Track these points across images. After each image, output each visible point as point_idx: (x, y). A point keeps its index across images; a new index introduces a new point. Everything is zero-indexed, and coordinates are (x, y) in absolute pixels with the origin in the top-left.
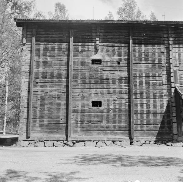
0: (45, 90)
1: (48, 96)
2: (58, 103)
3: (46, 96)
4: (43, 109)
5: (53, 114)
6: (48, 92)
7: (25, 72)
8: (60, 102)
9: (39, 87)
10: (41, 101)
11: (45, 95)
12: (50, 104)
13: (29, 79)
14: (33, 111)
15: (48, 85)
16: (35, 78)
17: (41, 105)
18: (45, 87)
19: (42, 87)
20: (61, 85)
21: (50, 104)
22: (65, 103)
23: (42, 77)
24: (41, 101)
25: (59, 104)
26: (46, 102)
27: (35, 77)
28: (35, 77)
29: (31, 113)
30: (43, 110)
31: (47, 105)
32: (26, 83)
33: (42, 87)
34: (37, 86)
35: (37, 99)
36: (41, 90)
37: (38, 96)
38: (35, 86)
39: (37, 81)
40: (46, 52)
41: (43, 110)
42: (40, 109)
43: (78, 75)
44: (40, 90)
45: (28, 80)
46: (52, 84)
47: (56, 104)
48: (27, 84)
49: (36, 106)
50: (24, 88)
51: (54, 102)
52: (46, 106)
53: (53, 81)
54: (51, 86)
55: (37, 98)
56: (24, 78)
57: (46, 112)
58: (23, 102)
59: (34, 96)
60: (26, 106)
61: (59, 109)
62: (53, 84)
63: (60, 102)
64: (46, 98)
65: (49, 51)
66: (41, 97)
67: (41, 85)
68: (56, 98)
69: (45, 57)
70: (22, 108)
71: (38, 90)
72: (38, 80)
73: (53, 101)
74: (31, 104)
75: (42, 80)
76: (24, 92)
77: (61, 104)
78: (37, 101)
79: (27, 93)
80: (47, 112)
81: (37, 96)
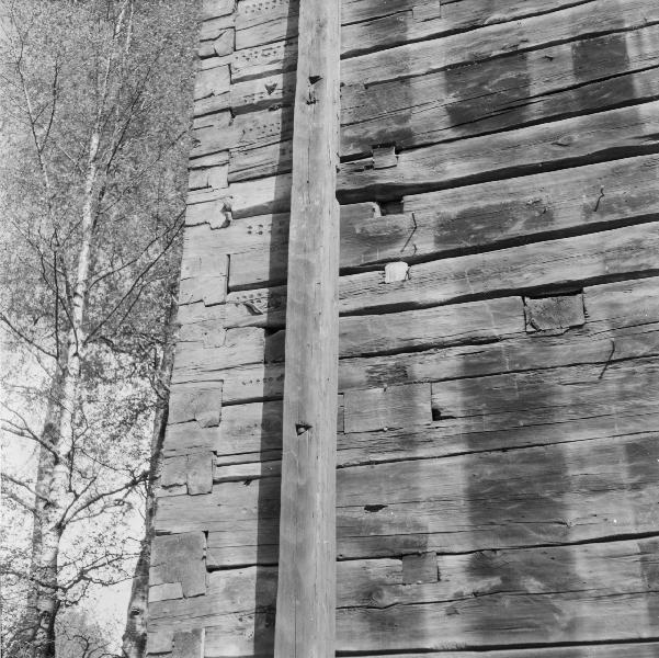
0: (525, 260)
1: (595, 345)
3: (563, 350)
6: (574, 288)
7: (234, 112)
9: (428, 248)
10: (472, 438)
11: (536, 335)
14: (355, 623)
15: (566, 195)
16: (359, 141)
17: (484, 502)
18: (517, 229)
19: (461, 238)
23: (463, 120)
24: (472, 438)
26: (577, 441)
27: (349, 133)
28: (349, 133)
30: (533, 585)
31: (600, 488)
32: (238, 227)
33: (461, 238)
34: (394, 238)
35: (409, 411)
36: (459, 276)
37: (422, 366)
39: (386, 178)
41: (533, 585)
42: (481, 565)
44: (442, 279)
46: (616, 173)
48: (254, 238)
49: (392, 521)
50: (217, 293)
52: (583, 515)
55: (409, 396)
56: (219, 177)
58: (201, 478)
59: (358, 371)
60: (238, 543)
64: (564, 388)
66: (471, 375)
67: (453, 211)
71: (422, 282)
72: (404, 168)
74: (302, 492)
76: (219, 337)
78: (408, 440)
79: (252, 345)
81: (402, 376)
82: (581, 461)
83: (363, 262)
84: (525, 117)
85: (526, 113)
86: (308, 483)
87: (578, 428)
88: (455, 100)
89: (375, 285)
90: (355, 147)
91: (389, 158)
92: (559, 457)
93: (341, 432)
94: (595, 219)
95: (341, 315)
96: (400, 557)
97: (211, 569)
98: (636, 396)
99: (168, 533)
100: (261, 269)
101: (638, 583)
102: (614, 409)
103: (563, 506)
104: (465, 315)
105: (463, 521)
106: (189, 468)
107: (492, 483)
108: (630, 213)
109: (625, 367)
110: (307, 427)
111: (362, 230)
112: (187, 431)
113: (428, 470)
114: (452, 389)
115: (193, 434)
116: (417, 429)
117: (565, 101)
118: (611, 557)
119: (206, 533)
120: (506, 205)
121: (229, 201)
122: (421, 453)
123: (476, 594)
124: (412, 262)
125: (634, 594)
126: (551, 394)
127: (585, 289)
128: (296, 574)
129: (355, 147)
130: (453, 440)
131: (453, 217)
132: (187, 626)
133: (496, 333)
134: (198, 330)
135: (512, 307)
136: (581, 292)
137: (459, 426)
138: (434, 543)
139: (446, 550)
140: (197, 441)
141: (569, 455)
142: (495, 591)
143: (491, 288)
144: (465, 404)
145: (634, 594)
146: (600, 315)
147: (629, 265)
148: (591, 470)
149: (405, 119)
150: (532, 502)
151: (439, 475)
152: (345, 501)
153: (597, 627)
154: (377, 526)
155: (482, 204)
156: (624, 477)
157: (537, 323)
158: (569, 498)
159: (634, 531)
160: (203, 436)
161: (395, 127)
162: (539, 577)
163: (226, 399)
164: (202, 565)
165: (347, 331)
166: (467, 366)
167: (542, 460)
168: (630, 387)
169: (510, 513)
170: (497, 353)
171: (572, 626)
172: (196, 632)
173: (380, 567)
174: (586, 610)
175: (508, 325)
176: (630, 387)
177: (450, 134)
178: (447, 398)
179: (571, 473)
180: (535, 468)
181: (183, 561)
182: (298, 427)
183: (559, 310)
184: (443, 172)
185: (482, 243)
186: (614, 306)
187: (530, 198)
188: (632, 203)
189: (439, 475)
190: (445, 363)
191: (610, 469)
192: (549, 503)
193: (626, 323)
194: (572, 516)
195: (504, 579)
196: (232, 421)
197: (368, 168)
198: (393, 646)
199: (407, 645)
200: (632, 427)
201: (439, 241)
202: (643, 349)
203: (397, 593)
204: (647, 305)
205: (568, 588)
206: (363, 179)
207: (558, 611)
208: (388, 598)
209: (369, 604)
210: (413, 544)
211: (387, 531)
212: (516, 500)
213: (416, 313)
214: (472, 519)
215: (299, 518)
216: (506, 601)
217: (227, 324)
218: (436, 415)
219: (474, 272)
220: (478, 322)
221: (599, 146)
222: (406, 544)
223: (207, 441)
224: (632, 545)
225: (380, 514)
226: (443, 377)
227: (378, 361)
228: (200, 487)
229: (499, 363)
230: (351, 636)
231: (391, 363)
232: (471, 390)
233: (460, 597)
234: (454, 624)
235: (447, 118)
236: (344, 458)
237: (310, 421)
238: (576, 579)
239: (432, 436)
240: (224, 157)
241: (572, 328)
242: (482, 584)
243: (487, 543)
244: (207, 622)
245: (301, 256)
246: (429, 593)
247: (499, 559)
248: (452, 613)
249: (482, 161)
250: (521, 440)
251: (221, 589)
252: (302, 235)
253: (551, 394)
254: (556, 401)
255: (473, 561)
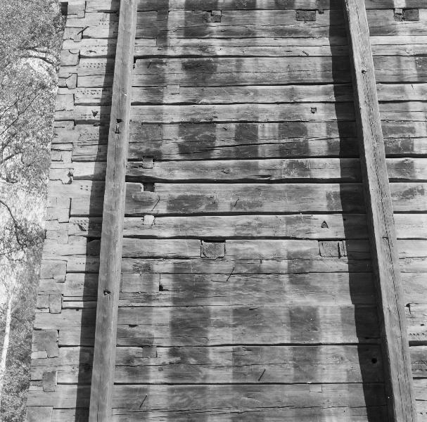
0: (204, 224)
1: (227, 266)
2: (298, 310)
3: (215, 267)
4: (193, 355)
5: (270, 394)
6: (222, 240)
7: (76, 123)
8: (309, 301)
9: (164, 211)
11: (205, 259)
12: (247, 316)
13: (101, 159)
14: (122, 372)
15: (224, 195)
17: (177, 327)
18: (202, 209)
19: (179, 207)
20: (310, 191)
21: (247, 316)
22: (344, 310)
23: (184, 151)
24: (175, 300)
25: (304, 320)
26: (216, 306)
27: (132, 147)
28: (132, 147)
29: (109, 385)
30: (192, 361)
31: (221, 325)
32: (76, 184)
33: (179, 207)
34: (149, 203)
35: (150, 286)
37: (158, 266)
38: (137, 207)
39: (148, 173)
40: (205, 19)
42: (174, 352)
43: (412, 130)
44: (168, 227)
45: (90, 169)
46: (246, 190)
47: (284, 318)
48: (83, 191)
49: (140, 332)
50: (65, 218)
51: (267, 306)
52: (215, 335)
53: (256, 168)
54: (246, 199)
55: (150, 279)
56: (67, 156)
57: (219, 374)
58: (56, 306)
59: (129, 264)
60: (73, 336)
61: (306, 351)
62: (258, 189)
63: (309, 301)
64: (213, 283)
65: (219, 13)
66: (177, 273)
67: (176, 195)
68: (285, 279)
69: (195, 41)
70: (41, 347)
72: (156, 169)
73: (260, 299)
75: (186, 169)
76: (66, 239)
77: (321, 313)
78: (149, 298)
79: (81, 245)
80: (226, 376)
81: (148, 269)
82: (216, 314)
83: (135, 212)
84: (211, 156)
85: (212, 154)
86: (107, 318)
87: (216, 301)
88: (182, 140)
89: (139, 225)
90: (135, 155)
91: (150, 164)
92: (208, 312)
93: (121, 292)
94: (234, 210)
95: (124, 237)
96: (142, 347)
97: (60, 346)
98: (240, 289)
99: (40, 330)
100: (85, 207)
101: (230, 363)
102: (232, 294)
103: (207, 331)
104: (177, 245)
105: (168, 334)
106: (50, 300)
107: (181, 320)
108: (248, 210)
109: (237, 277)
110: (109, 292)
111: (135, 197)
112: (49, 283)
113: (156, 312)
114: (168, 278)
115: (52, 285)
116: (153, 294)
117: (230, 152)
118: (222, 352)
119: (58, 331)
120: (199, 196)
121: (72, 171)
122: (154, 304)
123: (170, 363)
124: (156, 216)
125: (229, 367)
126: (207, 285)
127: (227, 241)
128: (102, 354)
129: (135, 155)
130: (167, 300)
131: (176, 198)
132: (50, 370)
133: (188, 254)
134: (55, 234)
135: (197, 244)
136: (224, 241)
137: (169, 294)
138: (156, 342)
139: (160, 345)
140: (54, 289)
141: (212, 311)
142: (179, 363)
143: (189, 235)
144: (173, 285)
145: (229, 367)
146: (230, 253)
147: (244, 233)
148: (219, 318)
149: (159, 145)
150: (196, 329)
151: (160, 314)
152: (121, 322)
153: (214, 378)
154: (133, 334)
155: (189, 194)
156: (231, 322)
157: (205, 253)
158: (209, 328)
159: (231, 343)
160: (57, 287)
161: (153, 149)
162: (196, 358)
163: (68, 270)
164: (57, 344)
165: (126, 245)
166: (175, 268)
167: (200, 312)
168: (238, 285)
169: (187, 333)
170: (186, 264)
171: (205, 378)
172: (54, 373)
173: (134, 350)
174: (211, 372)
175: (192, 251)
176: (238, 285)
177: (178, 157)
178: (166, 282)
179: (212, 318)
180: (198, 315)
181: (48, 342)
182: (105, 292)
183: (215, 248)
184: (174, 175)
185: (187, 213)
186: (236, 250)
187: (209, 195)
188: (251, 205)
189: (160, 314)
190: (167, 266)
191: (226, 318)
192: (201, 330)
193: (240, 258)
194: (210, 335)
195: (181, 358)
196: (71, 281)
197: (140, 166)
198: (136, 382)
199: (142, 382)
200: (236, 302)
201: (169, 208)
202: (245, 271)
203: (140, 361)
204: (248, 252)
205: (205, 363)
206: (137, 172)
207: (200, 371)
208: (136, 363)
209: (128, 364)
210: (148, 342)
211: (138, 336)
212: (189, 327)
213: (156, 241)
214: (172, 334)
215: (104, 331)
216: (182, 366)
217: (69, 234)
218: (161, 288)
219: (182, 226)
220: (181, 249)
221: (240, 177)
222: (145, 342)
223: (59, 289)
224: (230, 348)
225: (135, 329)
226: (165, 272)
227: (138, 261)
228: (56, 310)
229: (189, 269)
230: (120, 377)
231: (144, 263)
232: (176, 279)
233: (164, 364)
234: (161, 374)
235: (177, 149)
236: (122, 303)
237: (110, 290)
238: (209, 359)
239: (159, 297)
240: (70, 146)
241: (219, 257)
242: (173, 360)
243: (177, 344)
244: (58, 368)
245: (110, 212)
246: (152, 362)
247: (180, 350)
248: (161, 370)
249: (191, 173)
250: (193, 303)
251: (65, 355)
252: (110, 202)
253: (207, 285)
254: (209, 288)
255: (171, 350)
